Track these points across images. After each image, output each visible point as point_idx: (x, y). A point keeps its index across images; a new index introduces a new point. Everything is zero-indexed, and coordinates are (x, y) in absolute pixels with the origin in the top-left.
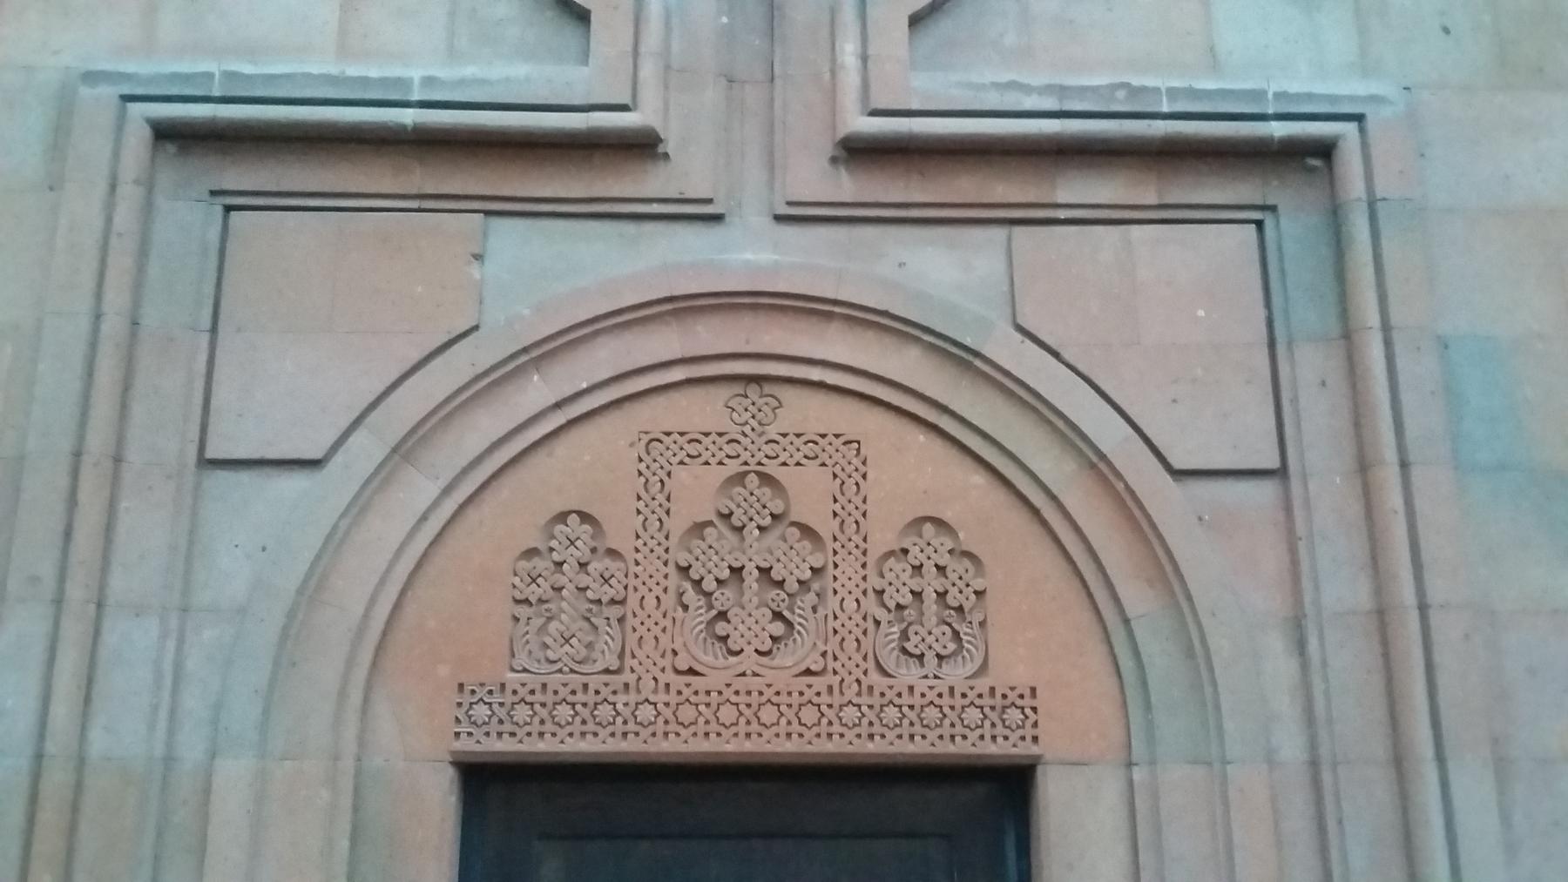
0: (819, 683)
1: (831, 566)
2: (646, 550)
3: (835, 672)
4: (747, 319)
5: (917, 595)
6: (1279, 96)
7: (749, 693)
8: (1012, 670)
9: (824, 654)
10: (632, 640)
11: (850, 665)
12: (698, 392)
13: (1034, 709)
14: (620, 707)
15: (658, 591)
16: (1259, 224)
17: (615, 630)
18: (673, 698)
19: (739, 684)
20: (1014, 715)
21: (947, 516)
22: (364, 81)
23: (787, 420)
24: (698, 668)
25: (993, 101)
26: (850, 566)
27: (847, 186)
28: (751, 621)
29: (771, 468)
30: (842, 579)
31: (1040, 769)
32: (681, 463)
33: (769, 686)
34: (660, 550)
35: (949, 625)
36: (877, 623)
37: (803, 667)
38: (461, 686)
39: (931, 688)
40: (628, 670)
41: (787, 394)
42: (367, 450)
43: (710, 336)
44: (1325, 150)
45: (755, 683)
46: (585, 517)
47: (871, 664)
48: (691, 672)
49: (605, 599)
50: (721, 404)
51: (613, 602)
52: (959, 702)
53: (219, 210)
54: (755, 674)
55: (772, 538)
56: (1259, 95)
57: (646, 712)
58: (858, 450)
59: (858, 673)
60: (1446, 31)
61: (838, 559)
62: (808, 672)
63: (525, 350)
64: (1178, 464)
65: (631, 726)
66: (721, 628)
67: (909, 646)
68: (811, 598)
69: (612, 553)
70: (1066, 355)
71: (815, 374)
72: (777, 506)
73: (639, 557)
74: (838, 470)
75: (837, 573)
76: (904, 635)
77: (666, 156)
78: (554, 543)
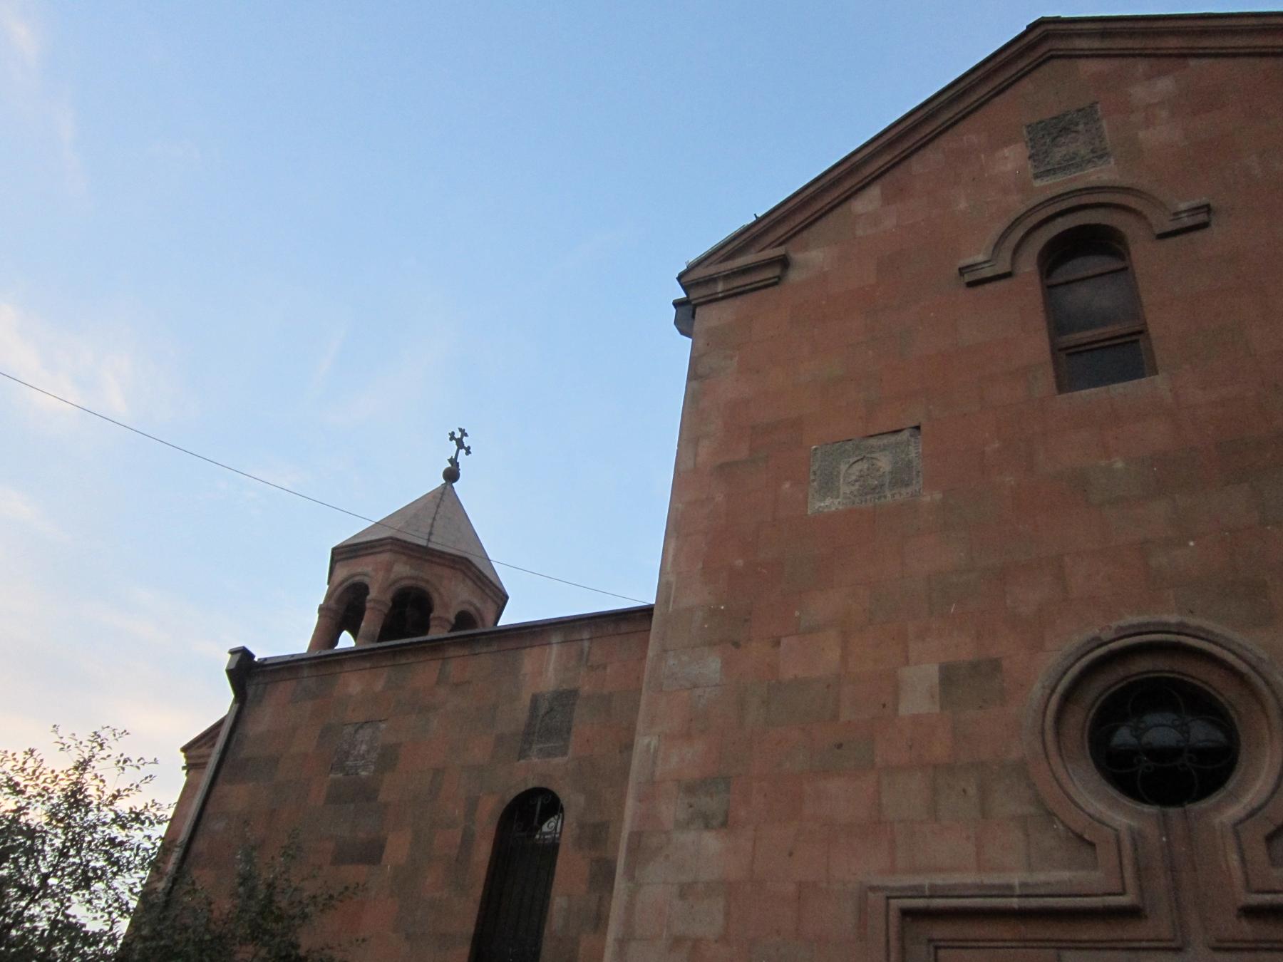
27: (1247, 929)
53: (932, 950)
77: (1146, 917)
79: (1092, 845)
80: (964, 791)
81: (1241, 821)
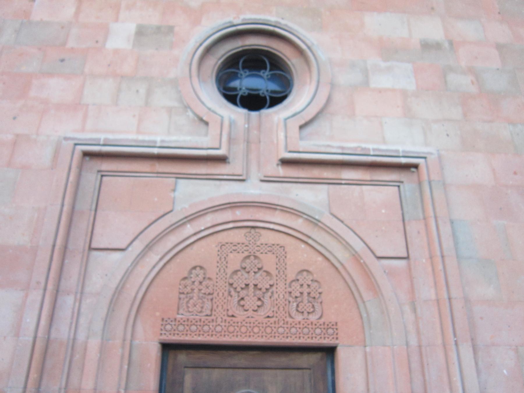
0: (272, 320)
1: (275, 284)
2: (219, 278)
3: (277, 317)
4: (251, 210)
5: (302, 293)
6: (403, 151)
7: (250, 323)
8: (330, 317)
9: (273, 311)
10: (215, 307)
11: (281, 315)
12: (237, 231)
13: (337, 329)
14: (211, 327)
15: (223, 291)
16: (399, 186)
17: (210, 303)
18: (227, 324)
19: (248, 320)
20: (330, 331)
21: (311, 269)
22: (144, 141)
23: (263, 240)
24: (235, 315)
25: (323, 150)
26: (281, 285)
28: (251, 302)
29: (258, 254)
30: (279, 288)
31: (339, 348)
32: (231, 252)
33: (256, 321)
34: (224, 279)
35: (311, 303)
36: (289, 302)
37: (267, 315)
38: (163, 319)
39: (306, 322)
40: (213, 315)
41: (263, 232)
42: (138, 246)
43: (239, 214)
44: (416, 166)
45: (252, 320)
46: (201, 268)
47: (287, 315)
48: (233, 316)
49: (207, 293)
50: (243, 235)
51: (209, 294)
52: (314, 327)
53: (99, 177)
54: (252, 317)
55: (258, 275)
56: (397, 151)
57: (219, 329)
58: (284, 250)
59: (284, 317)
60: (448, 135)
61: (278, 282)
62: (268, 317)
63: (186, 218)
64: (379, 254)
65: (214, 333)
66: (242, 303)
67: (299, 309)
68: (269, 294)
69: (210, 279)
70: (346, 222)
71: (272, 226)
72: (259, 266)
73: (218, 280)
74: (278, 255)
75: (278, 286)
76: (298, 306)
77: (229, 163)
78: (192, 276)
79: (207, 123)
80: (137, 91)
81: (289, 118)
